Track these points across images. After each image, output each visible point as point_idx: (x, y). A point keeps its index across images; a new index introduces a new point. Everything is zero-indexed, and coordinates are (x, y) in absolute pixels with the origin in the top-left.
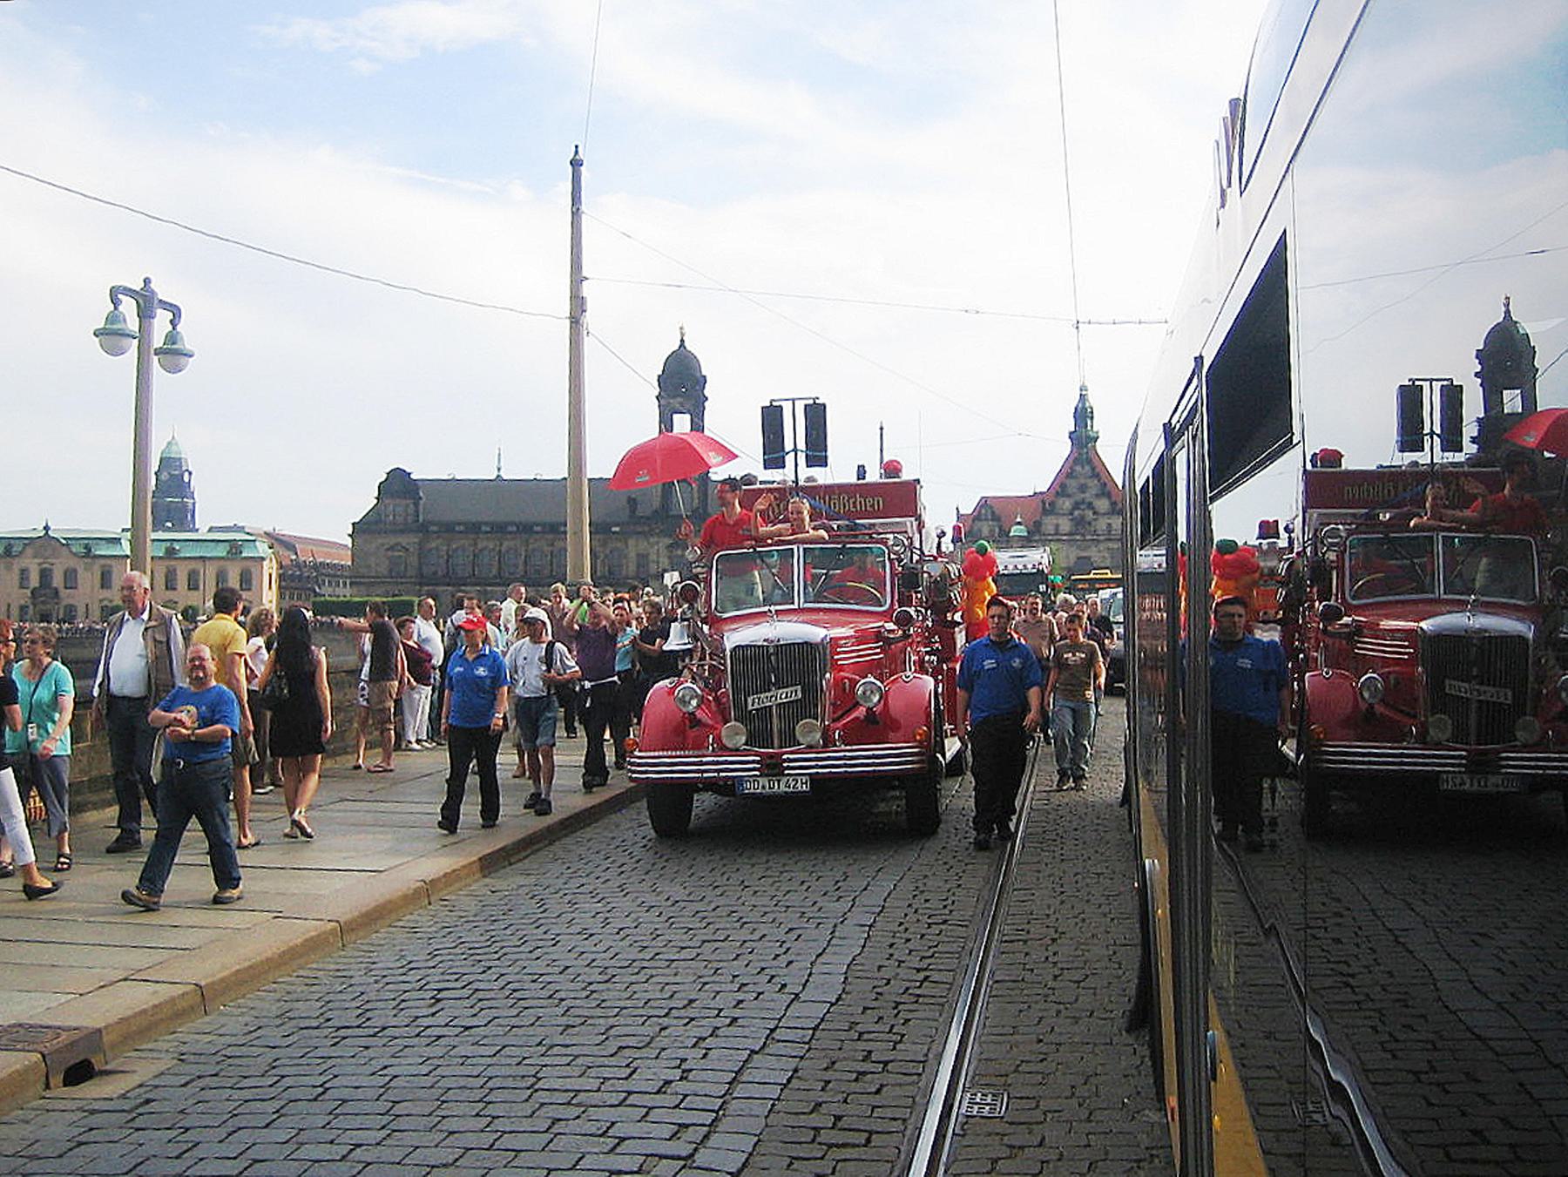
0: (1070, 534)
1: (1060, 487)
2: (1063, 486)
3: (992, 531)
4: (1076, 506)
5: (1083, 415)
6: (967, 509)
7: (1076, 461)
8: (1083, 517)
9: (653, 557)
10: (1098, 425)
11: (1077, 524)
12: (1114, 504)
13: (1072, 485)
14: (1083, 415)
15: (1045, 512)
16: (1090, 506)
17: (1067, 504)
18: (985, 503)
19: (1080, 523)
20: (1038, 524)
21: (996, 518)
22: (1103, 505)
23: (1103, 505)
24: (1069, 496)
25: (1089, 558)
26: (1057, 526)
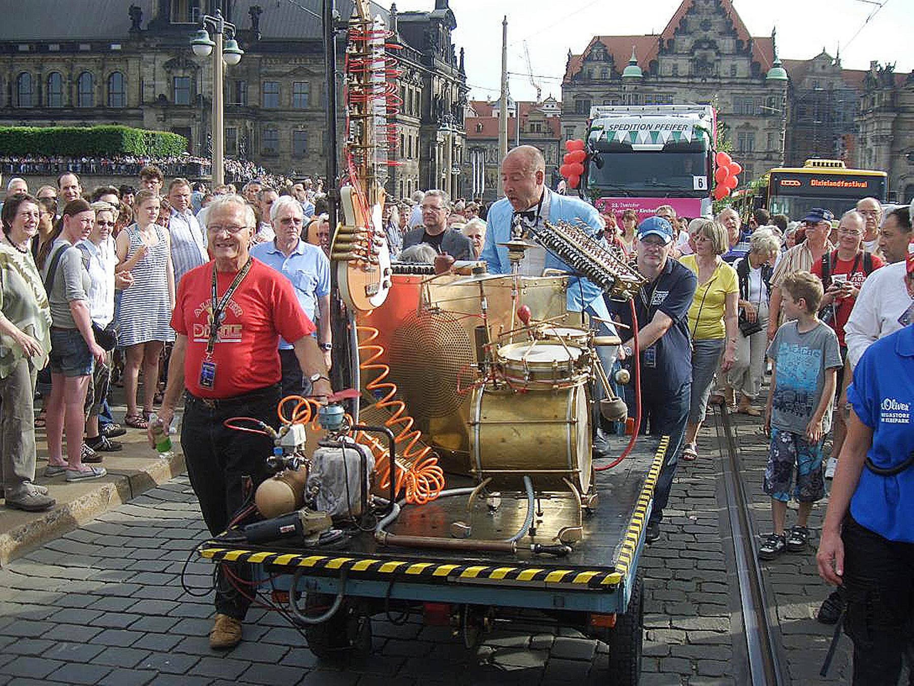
2: (683, 22)
4: (698, 45)
6: (579, 49)
9: (148, 79)
11: (696, 66)
12: (739, 43)
13: (694, 21)
15: (663, 51)
16: (712, 45)
17: (687, 42)
18: (597, 43)
19: (701, 65)
20: (654, 65)
21: (608, 58)
22: (727, 44)
23: (727, 44)
24: (690, 33)
26: (675, 67)
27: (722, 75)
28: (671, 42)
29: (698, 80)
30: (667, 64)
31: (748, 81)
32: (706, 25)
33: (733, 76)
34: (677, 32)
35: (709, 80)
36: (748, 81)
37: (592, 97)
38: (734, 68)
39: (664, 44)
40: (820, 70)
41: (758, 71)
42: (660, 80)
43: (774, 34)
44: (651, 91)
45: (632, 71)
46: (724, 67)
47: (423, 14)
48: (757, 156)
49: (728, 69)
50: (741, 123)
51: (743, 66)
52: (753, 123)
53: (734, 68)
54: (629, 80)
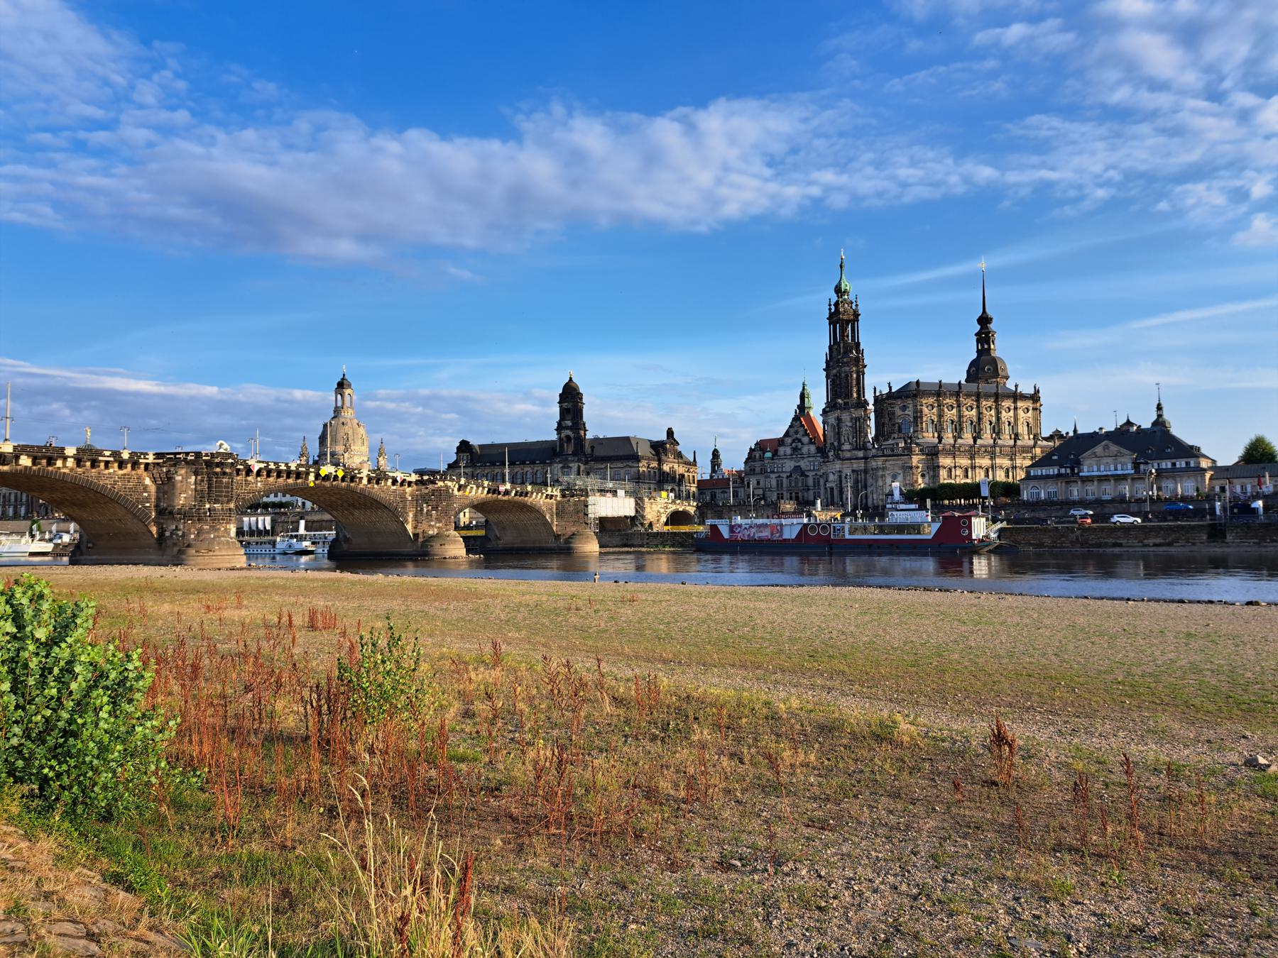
1: (787, 434)
4: (793, 441)
16: (800, 441)
17: (789, 440)
19: (795, 450)
22: (805, 440)
30: (781, 450)
32: (797, 432)
46: (805, 450)
51: (813, 448)
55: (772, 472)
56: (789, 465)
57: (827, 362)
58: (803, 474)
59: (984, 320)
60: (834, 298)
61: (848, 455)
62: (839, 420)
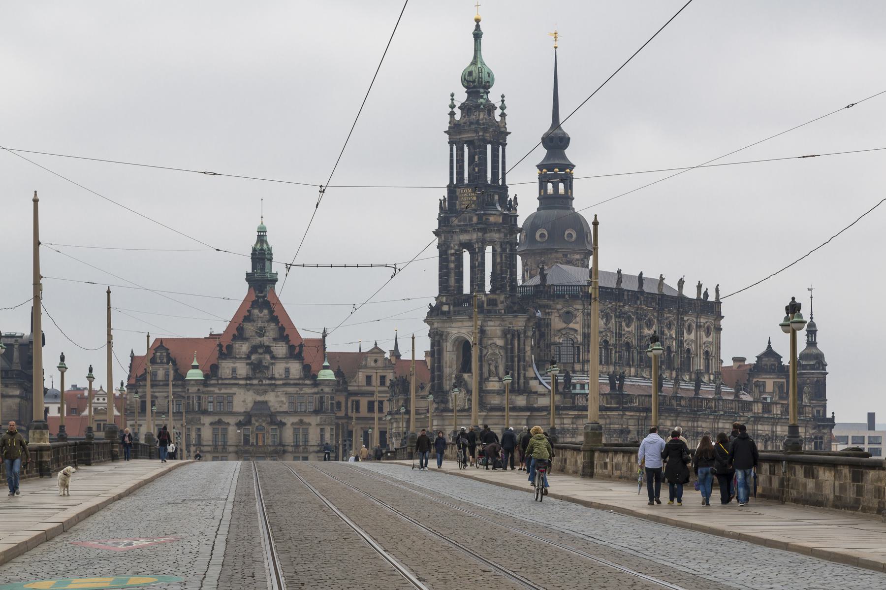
0: (247, 378)
2: (240, 329)
3: (167, 375)
4: (254, 349)
5: (261, 256)
7: (255, 304)
8: (260, 361)
10: (277, 267)
11: (254, 370)
12: (291, 348)
13: (250, 328)
14: (261, 256)
16: (268, 350)
17: (243, 348)
19: (257, 368)
20: (215, 368)
22: (280, 349)
23: (280, 349)
24: (247, 339)
25: (266, 402)
26: (234, 370)
27: (277, 376)
28: (230, 347)
29: (255, 382)
30: (226, 368)
31: (301, 382)
32: (261, 332)
33: (287, 377)
34: (235, 338)
35: (266, 382)
36: (301, 382)
37: (157, 397)
38: (287, 370)
39: (222, 347)
40: (373, 364)
41: (309, 373)
42: (220, 382)
43: (325, 335)
44: (213, 393)
45: (194, 374)
46: (279, 369)
47: (21, 337)
48: (311, 449)
49: (282, 371)
50: (295, 419)
51: (295, 368)
52: (306, 419)
53: (287, 370)
54: (193, 382)
55: (205, 412)
56: (243, 400)
57: (444, 221)
58: (274, 420)
59: (556, 142)
60: (462, 96)
61: (495, 401)
62: (482, 332)
